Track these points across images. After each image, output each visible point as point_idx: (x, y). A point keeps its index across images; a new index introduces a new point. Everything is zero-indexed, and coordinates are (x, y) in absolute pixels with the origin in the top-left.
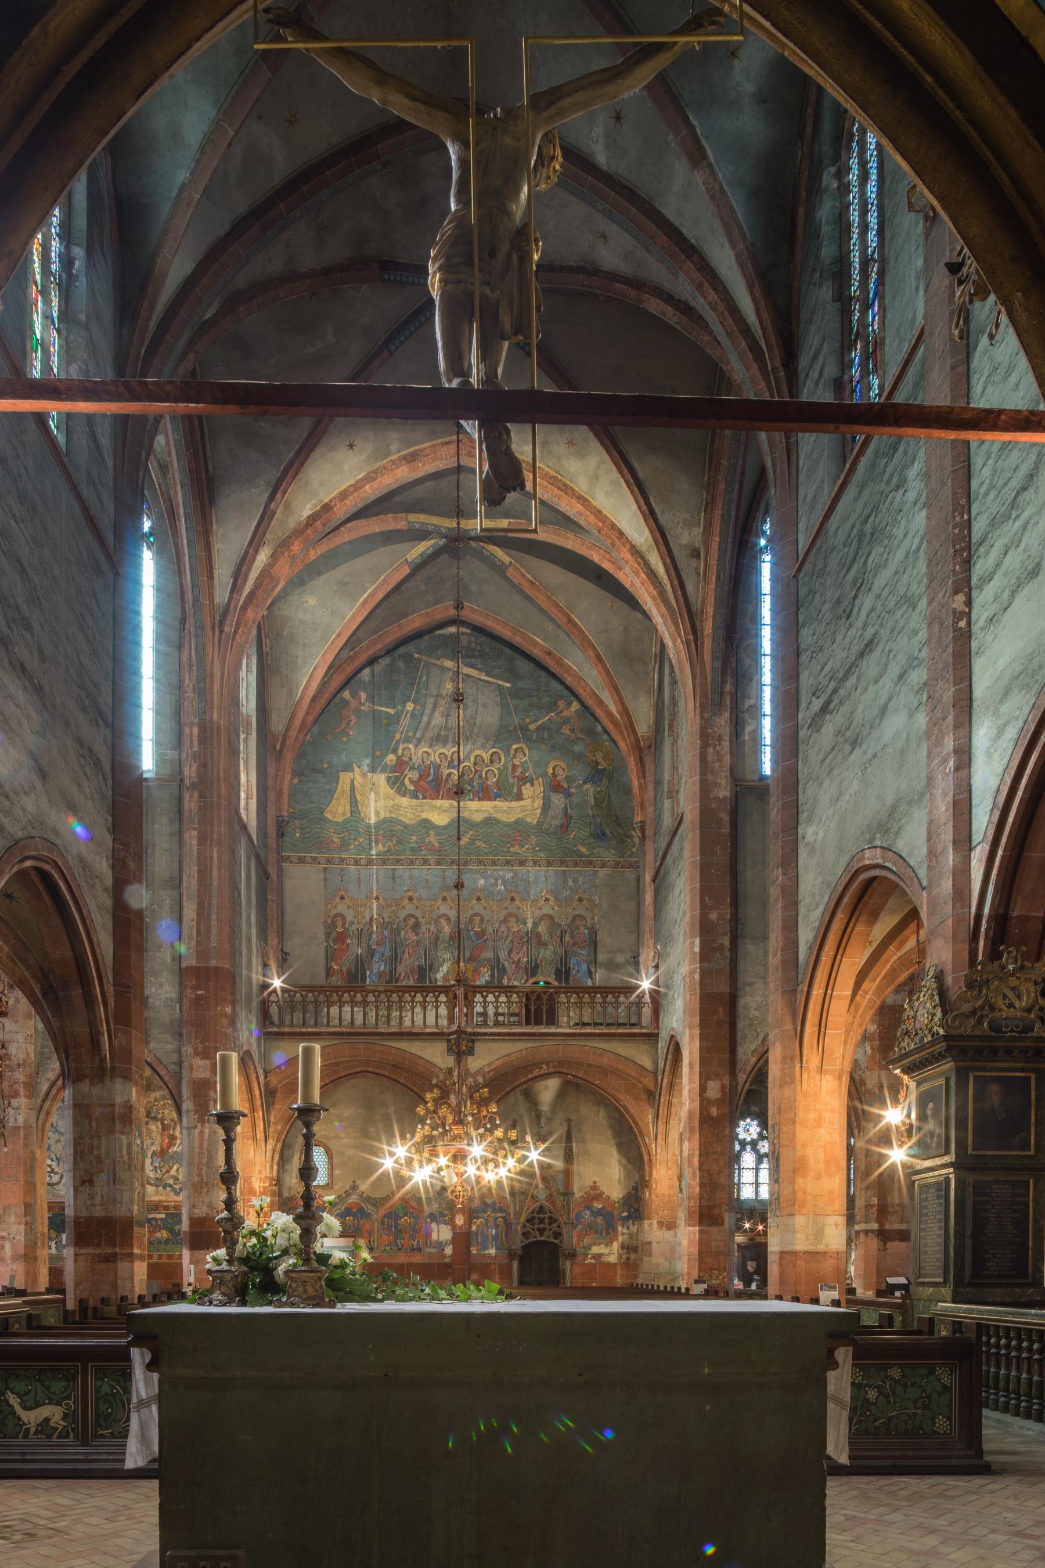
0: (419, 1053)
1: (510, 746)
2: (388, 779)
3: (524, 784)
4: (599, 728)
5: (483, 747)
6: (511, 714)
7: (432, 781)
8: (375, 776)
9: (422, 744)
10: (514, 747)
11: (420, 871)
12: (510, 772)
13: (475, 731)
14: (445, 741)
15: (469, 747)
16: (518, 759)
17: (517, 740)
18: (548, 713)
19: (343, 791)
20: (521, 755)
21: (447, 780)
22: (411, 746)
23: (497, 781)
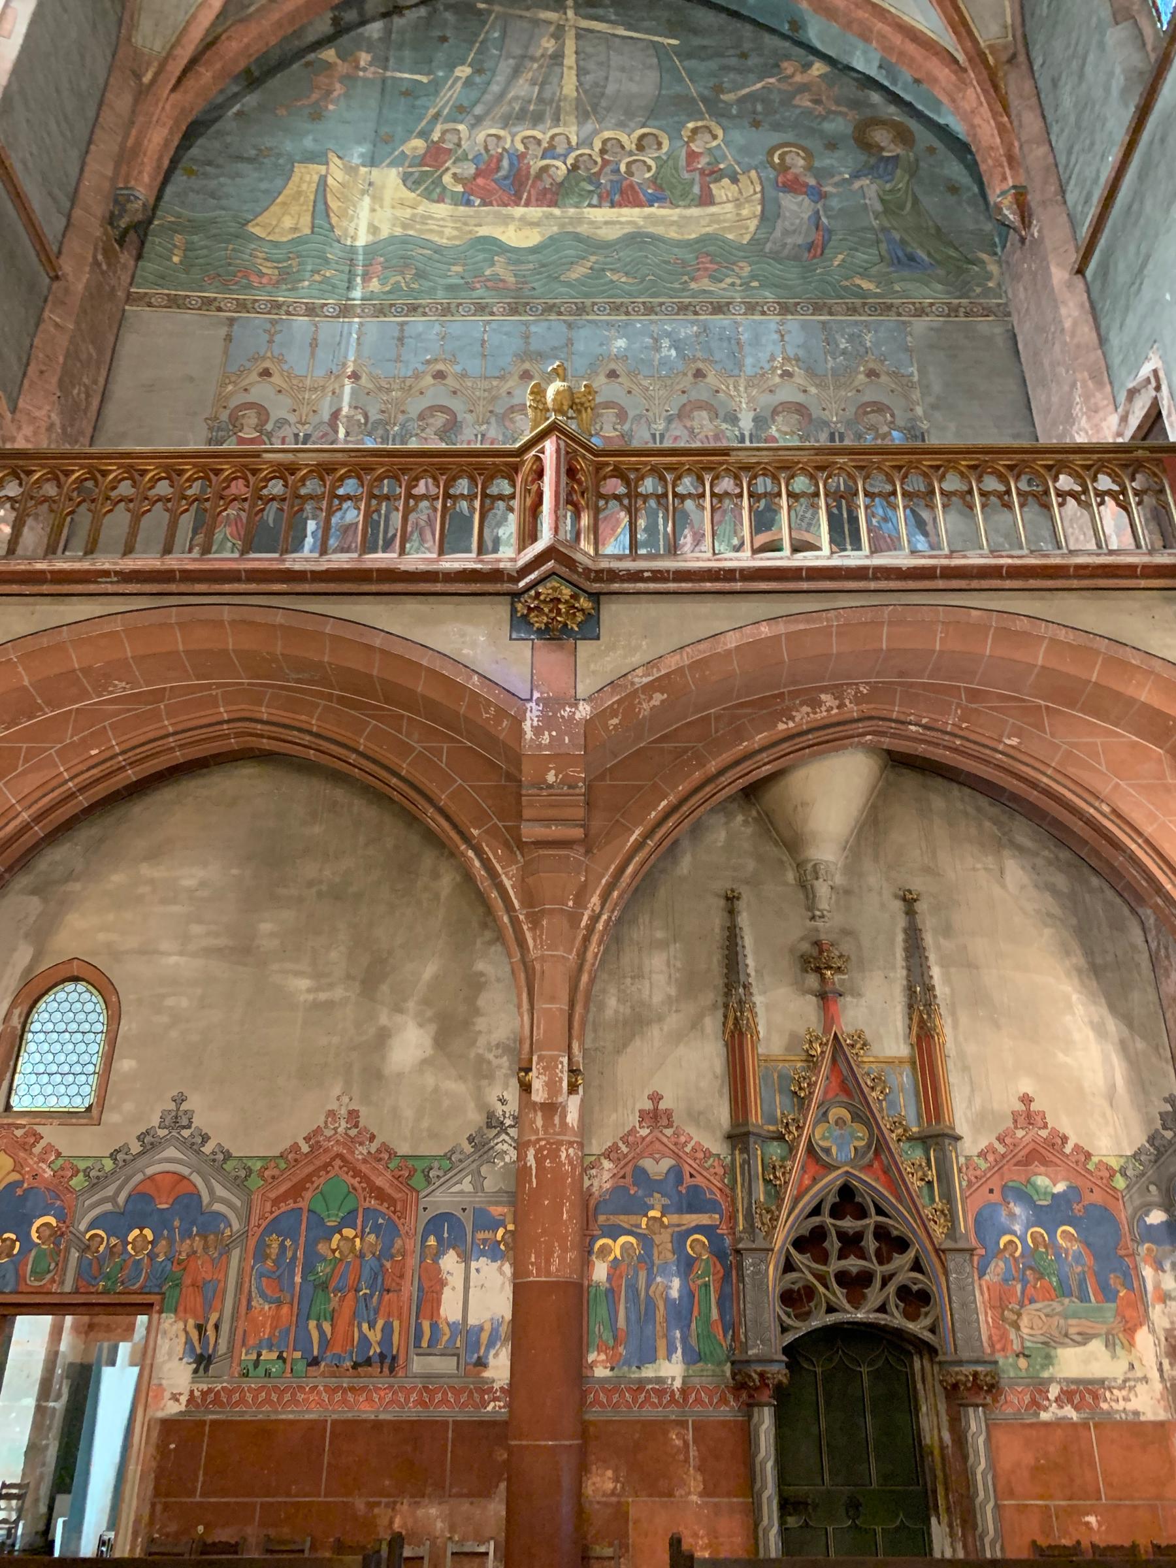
0: (419, 635)
1: (683, 125)
2: (405, 178)
3: (717, 180)
4: (876, 97)
5: (621, 125)
6: (681, 80)
7: (506, 178)
8: (375, 171)
9: (486, 123)
10: (691, 125)
11: (469, 326)
12: (682, 162)
13: (604, 103)
14: (537, 119)
15: (590, 126)
16: (698, 142)
17: (691, 117)
18: (761, 79)
19: (299, 193)
20: (708, 137)
21: (538, 176)
22: (461, 127)
23: (655, 177)
